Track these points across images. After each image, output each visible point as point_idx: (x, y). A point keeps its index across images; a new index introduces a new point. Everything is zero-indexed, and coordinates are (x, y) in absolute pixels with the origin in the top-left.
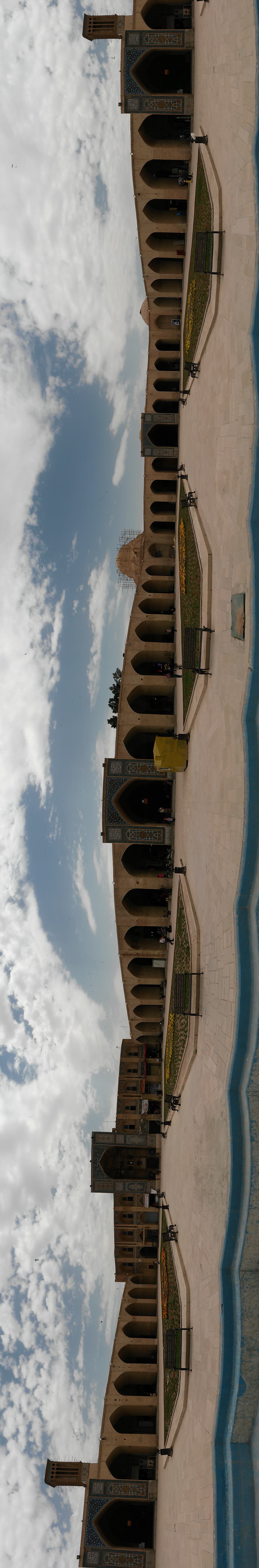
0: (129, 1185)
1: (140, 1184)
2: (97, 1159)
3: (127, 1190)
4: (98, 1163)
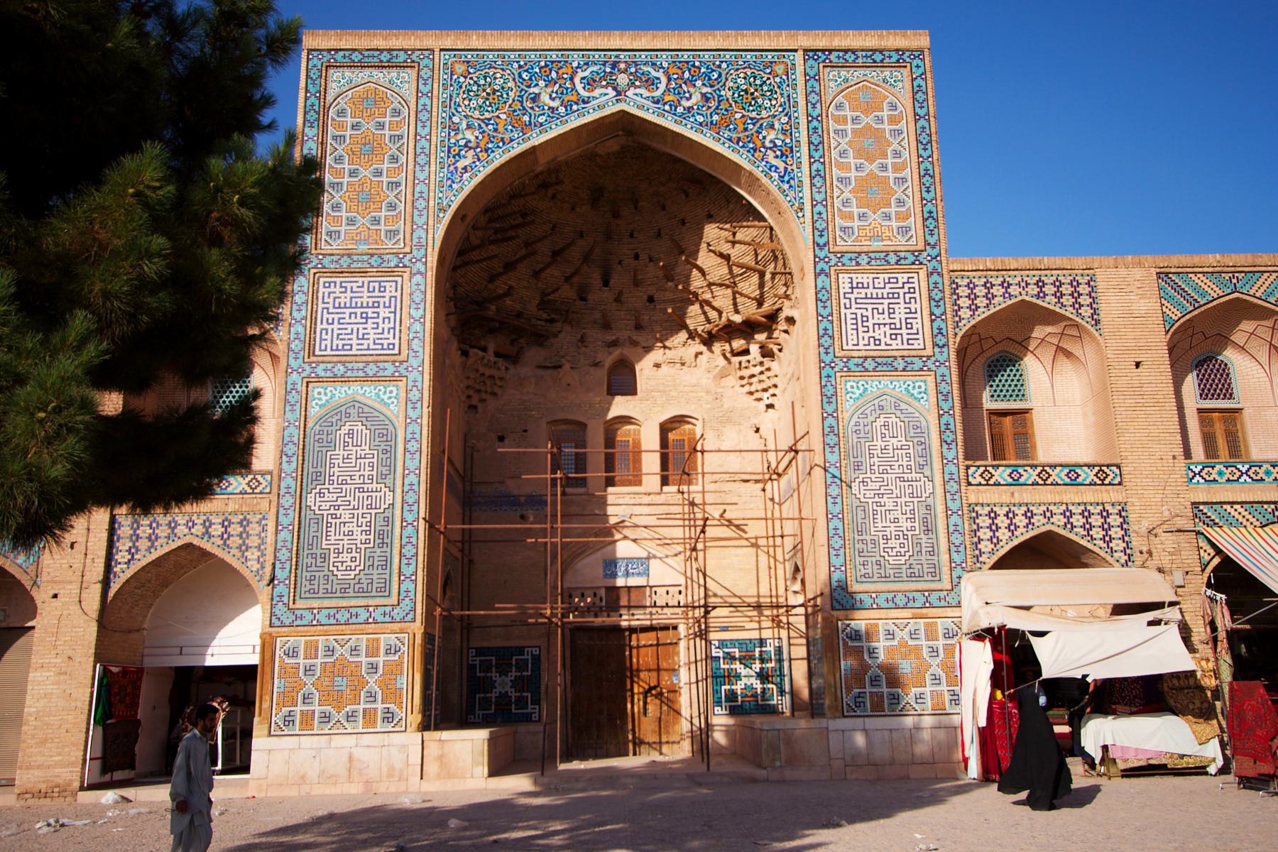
0: (365, 414)
1: (383, 539)
2: (650, 83)
3: (323, 397)
4: (603, 104)
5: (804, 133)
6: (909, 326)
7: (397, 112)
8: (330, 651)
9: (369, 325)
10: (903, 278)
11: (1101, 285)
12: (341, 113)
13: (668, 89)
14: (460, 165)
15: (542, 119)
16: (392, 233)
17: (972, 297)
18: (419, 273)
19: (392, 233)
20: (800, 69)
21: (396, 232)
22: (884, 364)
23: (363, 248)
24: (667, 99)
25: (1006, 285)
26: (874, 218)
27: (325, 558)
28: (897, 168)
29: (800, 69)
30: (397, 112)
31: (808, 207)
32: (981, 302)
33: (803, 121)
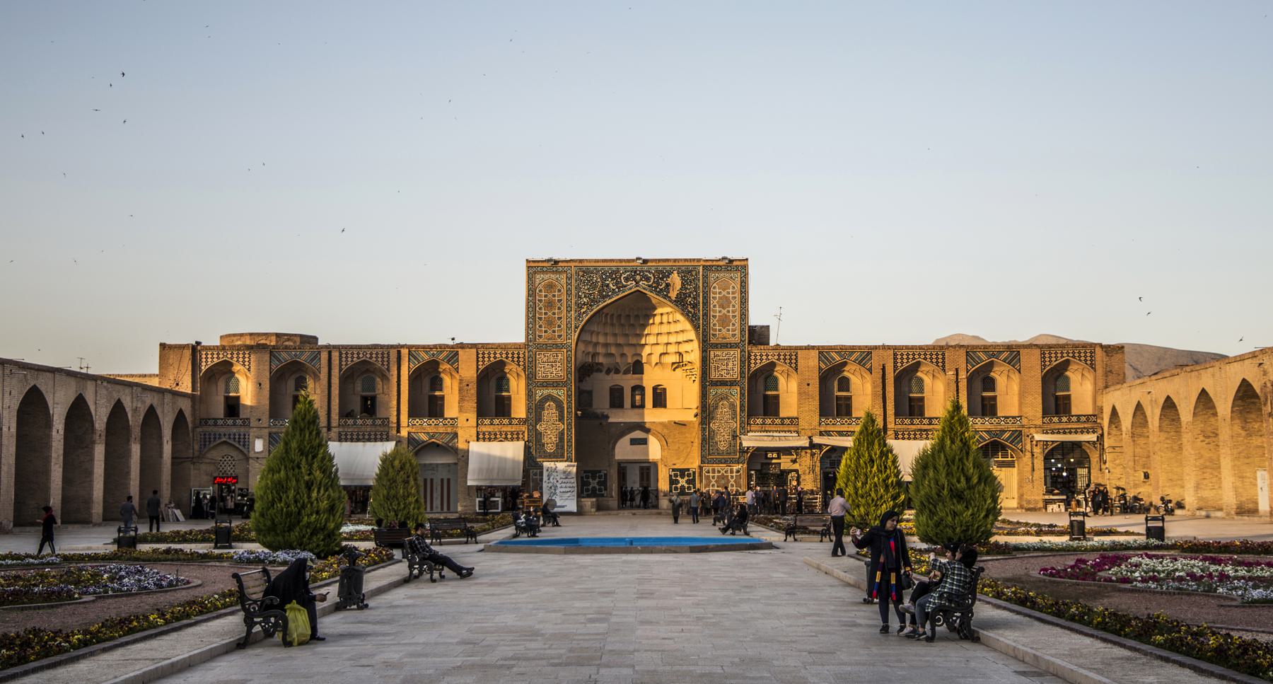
2: (648, 279)
5: (701, 299)
6: (733, 370)
7: (559, 291)
10: (732, 353)
11: (799, 356)
12: (540, 291)
13: (654, 282)
14: (582, 311)
15: (610, 294)
16: (560, 336)
17: (756, 359)
18: (569, 351)
19: (560, 336)
20: (701, 273)
21: (561, 336)
22: (723, 383)
24: (654, 285)
25: (767, 355)
26: (724, 331)
27: (543, 445)
28: (733, 312)
29: (701, 273)
30: (559, 291)
31: (701, 327)
32: (758, 361)
33: (701, 294)
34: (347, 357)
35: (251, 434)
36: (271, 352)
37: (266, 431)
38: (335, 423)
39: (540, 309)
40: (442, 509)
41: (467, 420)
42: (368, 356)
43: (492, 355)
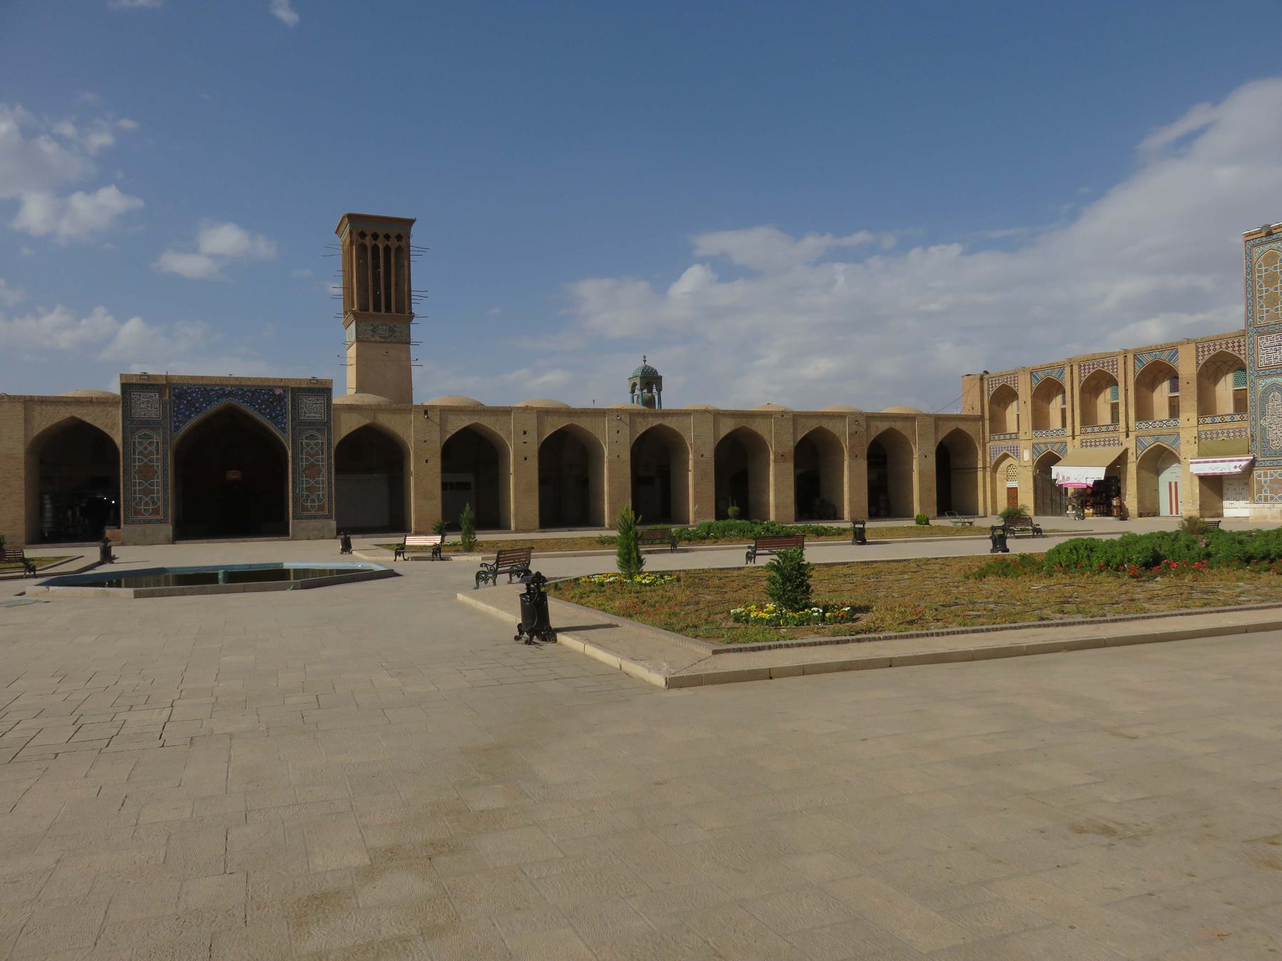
8: (1272, 475)
9: (1277, 353)
12: (1260, 266)
23: (1273, 322)
27: (1268, 442)
34: (1085, 369)
35: (1021, 446)
36: (1031, 373)
37: (1029, 444)
38: (1077, 432)
39: (1261, 286)
40: (1171, 513)
41: (1188, 420)
42: (1101, 365)
43: (1212, 348)
